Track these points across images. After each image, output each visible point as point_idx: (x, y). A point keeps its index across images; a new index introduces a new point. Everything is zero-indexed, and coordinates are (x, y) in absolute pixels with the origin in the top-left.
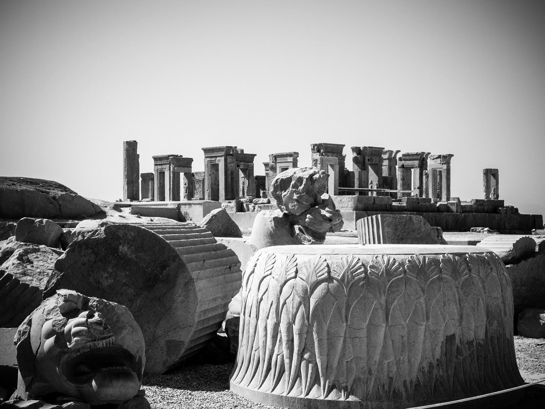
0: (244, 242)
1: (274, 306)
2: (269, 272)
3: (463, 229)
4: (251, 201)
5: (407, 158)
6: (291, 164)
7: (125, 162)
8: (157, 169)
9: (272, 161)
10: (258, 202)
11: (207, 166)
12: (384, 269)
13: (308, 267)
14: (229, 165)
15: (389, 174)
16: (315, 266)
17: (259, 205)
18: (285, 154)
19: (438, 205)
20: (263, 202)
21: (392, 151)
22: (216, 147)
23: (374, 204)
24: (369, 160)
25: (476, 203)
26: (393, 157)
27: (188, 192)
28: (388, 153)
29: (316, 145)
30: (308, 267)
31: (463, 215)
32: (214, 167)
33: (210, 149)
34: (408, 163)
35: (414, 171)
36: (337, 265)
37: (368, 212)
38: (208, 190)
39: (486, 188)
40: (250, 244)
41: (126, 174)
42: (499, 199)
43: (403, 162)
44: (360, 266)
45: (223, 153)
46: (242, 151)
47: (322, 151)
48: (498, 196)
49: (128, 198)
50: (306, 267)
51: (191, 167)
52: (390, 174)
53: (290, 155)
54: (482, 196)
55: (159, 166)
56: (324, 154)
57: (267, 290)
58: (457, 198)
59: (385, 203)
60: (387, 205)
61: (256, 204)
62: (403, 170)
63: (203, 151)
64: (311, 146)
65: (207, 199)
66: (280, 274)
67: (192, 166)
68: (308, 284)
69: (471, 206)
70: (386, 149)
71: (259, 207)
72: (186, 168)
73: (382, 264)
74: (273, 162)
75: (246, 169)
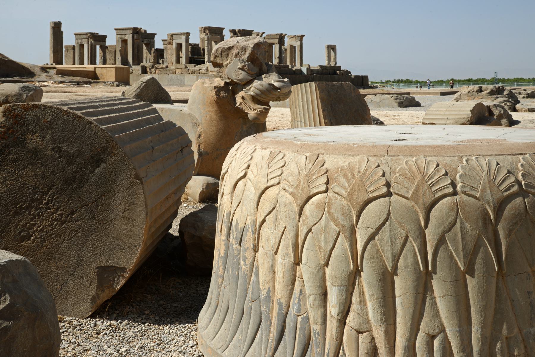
0: (181, 111)
1: (289, 236)
2: (276, 181)
4: (153, 66)
12: (486, 180)
13: (350, 176)
16: (361, 174)
19: (294, 69)
20: (163, 67)
27: (103, 60)
30: (350, 176)
31: (312, 76)
36: (401, 173)
40: (187, 113)
42: (337, 65)
44: (443, 175)
48: (336, 63)
50: (345, 176)
54: (325, 63)
57: (274, 208)
61: (157, 68)
65: (118, 65)
66: (299, 185)
68: (353, 204)
69: (318, 70)
71: (159, 70)
73: (480, 172)
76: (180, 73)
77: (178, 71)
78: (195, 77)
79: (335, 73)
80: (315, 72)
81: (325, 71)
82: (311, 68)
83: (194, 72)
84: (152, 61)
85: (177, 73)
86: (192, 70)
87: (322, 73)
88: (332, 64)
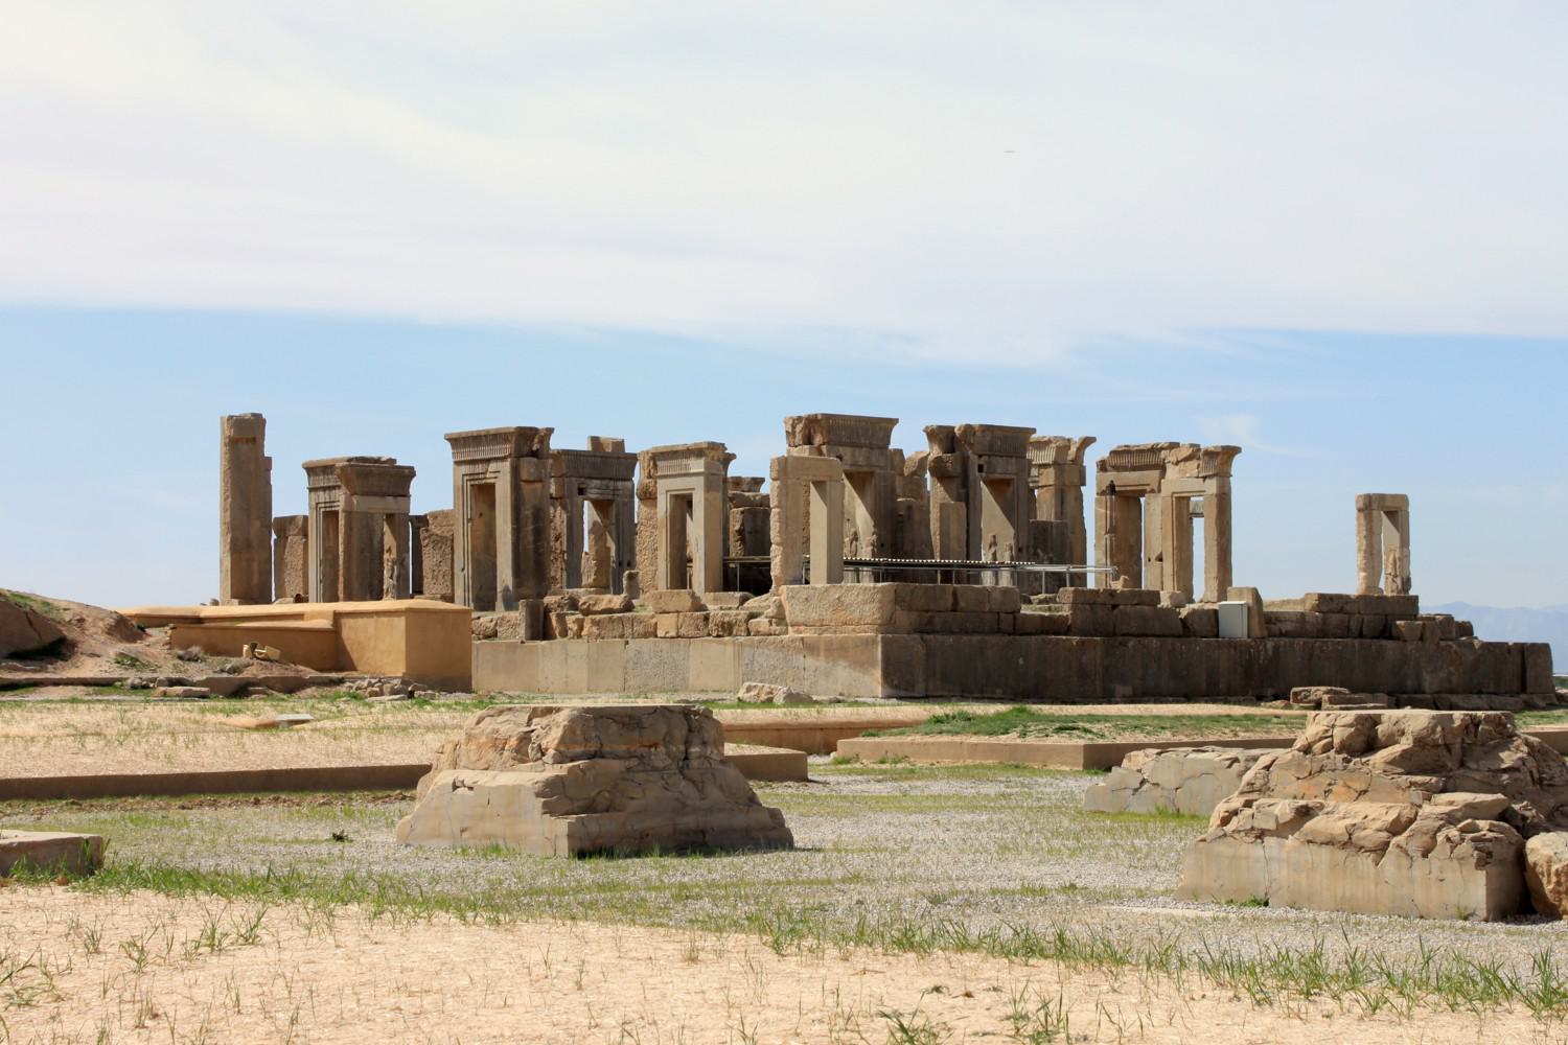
3: (1270, 692)
5: (1124, 460)
6: (702, 478)
7: (225, 481)
8: (317, 504)
9: (647, 471)
10: (596, 608)
11: (459, 491)
14: (526, 489)
15: (1056, 513)
17: (594, 617)
18: (680, 448)
19: (1184, 612)
20: (612, 606)
21: (1069, 440)
22: (488, 431)
23: (954, 610)
24: (981, 468)
26: (1070, 458)
27: (398, 577)
28: (1053, 445)
29: (799, 419)
32: (484, 493)
33: (468, 437)
34: (1127, 479)
35: (1148, 504)
37: (927, 637)
38: (463, 570)
39: (1365, 558)
41: (228, 519)
43: (1111, 476)
45: (506, 449)
46: (620, 445)
47: (818, 439)
48: (1407, 583)
49: (233, 597)
51: (406, 495)
52: (1062, 513)
53: (696, 452)
54: (1350, 584)
55: (321, 493)
56: (824, 448)
58: (1248, 589)
59: (995, 607)
60: (1003, 615)
61: (587, 612)
62: (1111, 499)
63: (448, 444)
64: (786, 423)
67: (411, 491)
69: (1303, 614)
70: (1042, 433)
71: (596, 623)
74: (649, 476)
75: (610, 502)
76: (673, 634)
77: (667, 624)
78: (730, 649)
79: (1386, 632)
81: (1335, 619)
82: (1265, 610)
83: (727, 629)
84: (591, 580)
85: (660, 633)
86: (718, 619)
87: (1323, 633)
88: (1386, 586)
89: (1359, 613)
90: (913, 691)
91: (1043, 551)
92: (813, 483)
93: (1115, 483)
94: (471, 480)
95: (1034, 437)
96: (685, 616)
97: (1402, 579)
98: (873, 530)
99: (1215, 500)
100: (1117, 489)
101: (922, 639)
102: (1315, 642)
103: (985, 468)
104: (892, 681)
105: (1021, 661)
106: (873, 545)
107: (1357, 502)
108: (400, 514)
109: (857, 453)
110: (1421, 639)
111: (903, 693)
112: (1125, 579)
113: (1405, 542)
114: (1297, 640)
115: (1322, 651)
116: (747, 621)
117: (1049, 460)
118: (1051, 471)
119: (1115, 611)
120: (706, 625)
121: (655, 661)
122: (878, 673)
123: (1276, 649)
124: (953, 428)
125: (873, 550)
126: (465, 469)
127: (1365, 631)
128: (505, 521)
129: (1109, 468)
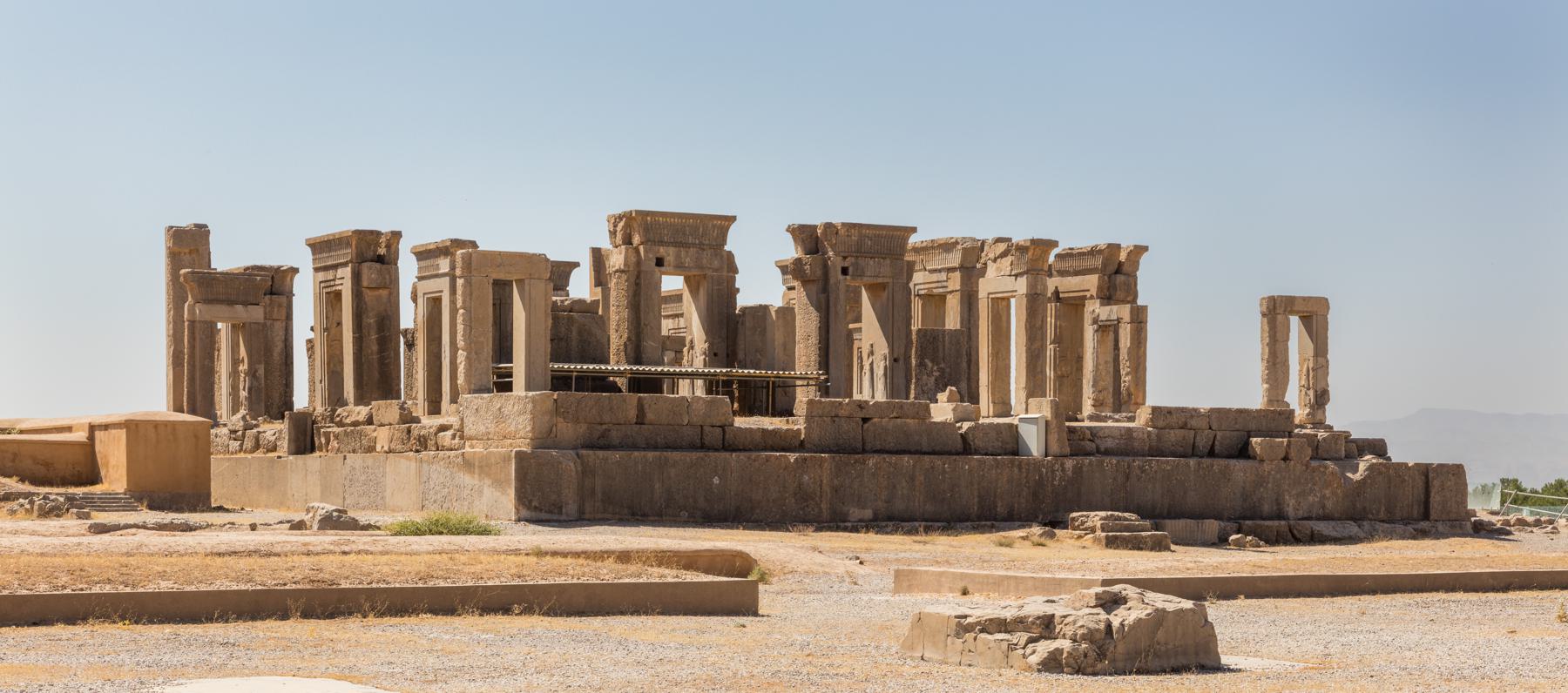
14: (369, 296)
22: (334, 235)
24: (845, 271)
25: (1151, 419)
39: (1268, 368)
63: (309, 250)
72: (239, 308)
80: (1110, 443)
89: (1210, 428)
90: (560, 513)
91: (932, 361)
92: (516, 280)
93: (1060, 289)
94: (325, 287)
95: (914, 240)
96: (395, 428)
97: (1316, 391)
98: (705, 338)
99: (1025, 299)
100: (1061, 295)
101: (578, 455)
102: (1134, 461)
103: (851, 270)
104: (530, 501)
105: (716, 480)
106: (705, 353)
107: (1261, 305)
108: (250, 323)
109: (683, 254)
110: (1286, 459)
111: (544, 516)
112: (951, 390)
113: (1321, 350)
114: (1107, 459)
115: (1143, 471)
116: (436, 434)
117: (956, 264)
118: (958, 274)
119: (866, 426)
120: (409, 439)
121: (363, 478)
122: (512, 492)
123: (1078, 470)
124: (815, 227)
125: (705, 359)
126: (321, 276)
127: (1217, 448)
128: (348, 330)
129: (1055, 273)
